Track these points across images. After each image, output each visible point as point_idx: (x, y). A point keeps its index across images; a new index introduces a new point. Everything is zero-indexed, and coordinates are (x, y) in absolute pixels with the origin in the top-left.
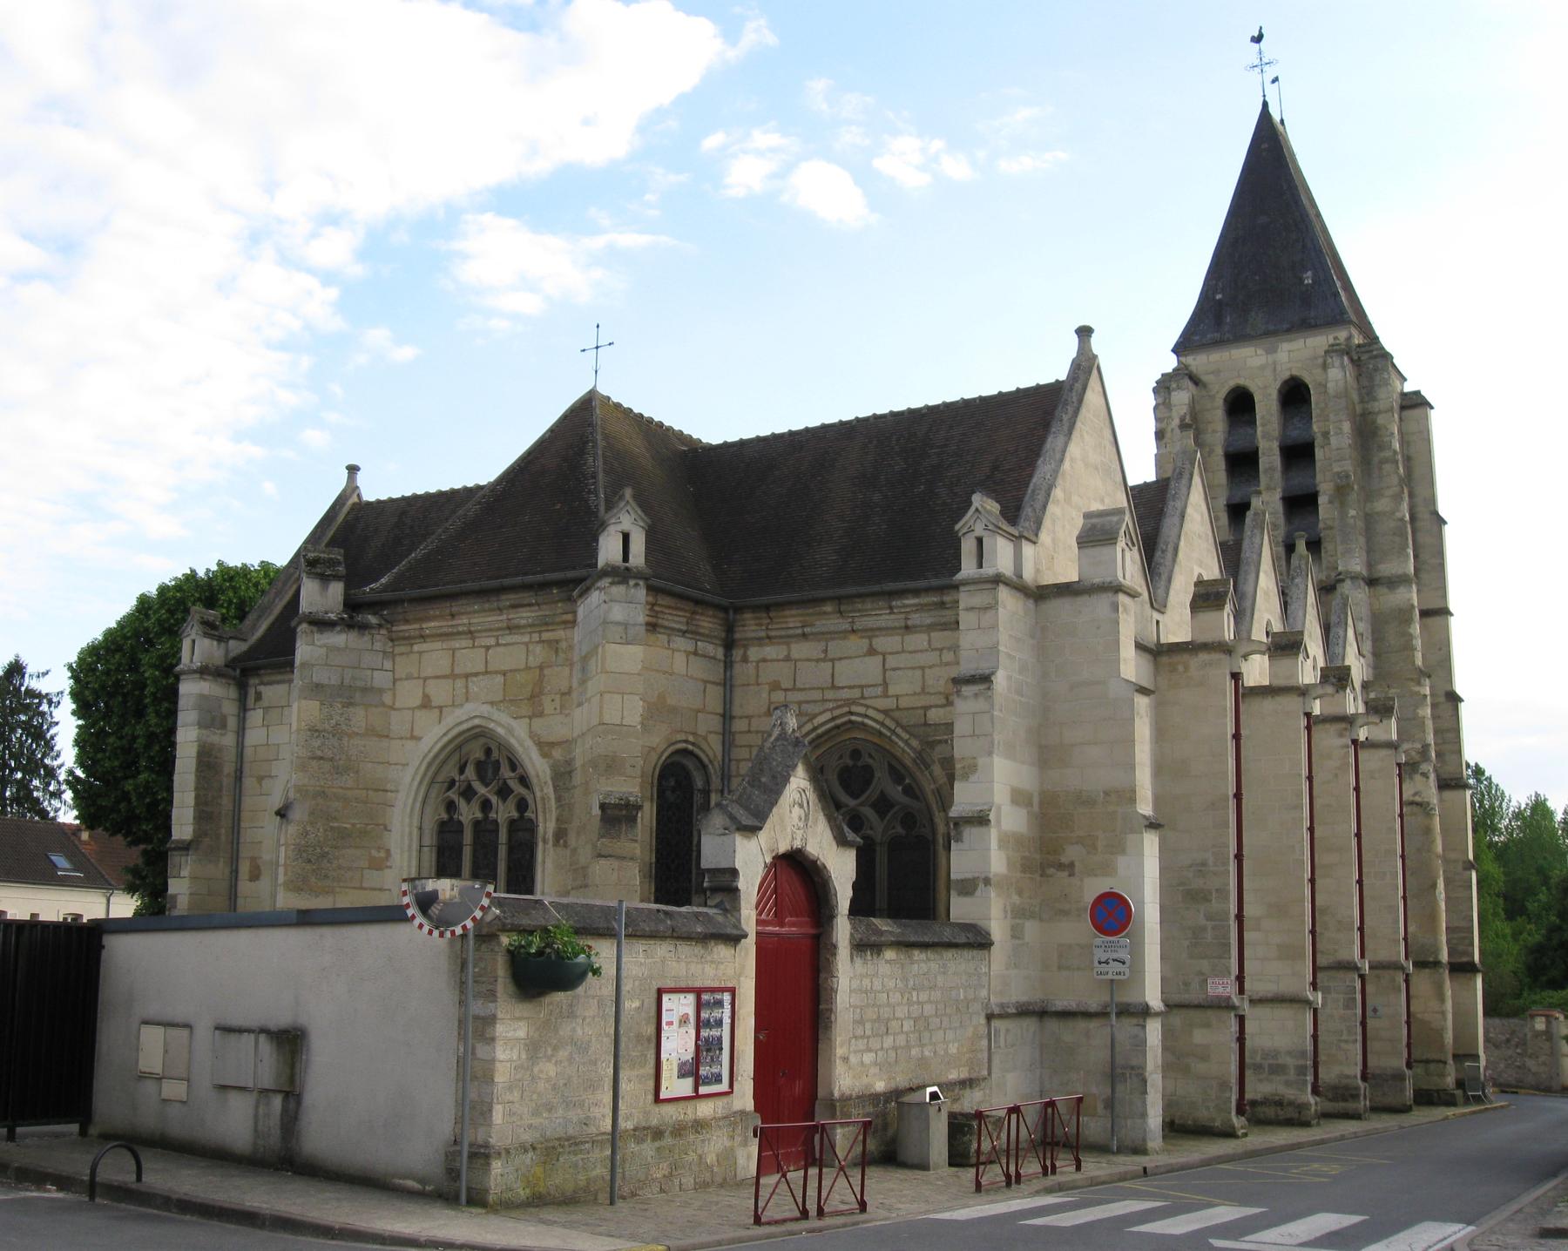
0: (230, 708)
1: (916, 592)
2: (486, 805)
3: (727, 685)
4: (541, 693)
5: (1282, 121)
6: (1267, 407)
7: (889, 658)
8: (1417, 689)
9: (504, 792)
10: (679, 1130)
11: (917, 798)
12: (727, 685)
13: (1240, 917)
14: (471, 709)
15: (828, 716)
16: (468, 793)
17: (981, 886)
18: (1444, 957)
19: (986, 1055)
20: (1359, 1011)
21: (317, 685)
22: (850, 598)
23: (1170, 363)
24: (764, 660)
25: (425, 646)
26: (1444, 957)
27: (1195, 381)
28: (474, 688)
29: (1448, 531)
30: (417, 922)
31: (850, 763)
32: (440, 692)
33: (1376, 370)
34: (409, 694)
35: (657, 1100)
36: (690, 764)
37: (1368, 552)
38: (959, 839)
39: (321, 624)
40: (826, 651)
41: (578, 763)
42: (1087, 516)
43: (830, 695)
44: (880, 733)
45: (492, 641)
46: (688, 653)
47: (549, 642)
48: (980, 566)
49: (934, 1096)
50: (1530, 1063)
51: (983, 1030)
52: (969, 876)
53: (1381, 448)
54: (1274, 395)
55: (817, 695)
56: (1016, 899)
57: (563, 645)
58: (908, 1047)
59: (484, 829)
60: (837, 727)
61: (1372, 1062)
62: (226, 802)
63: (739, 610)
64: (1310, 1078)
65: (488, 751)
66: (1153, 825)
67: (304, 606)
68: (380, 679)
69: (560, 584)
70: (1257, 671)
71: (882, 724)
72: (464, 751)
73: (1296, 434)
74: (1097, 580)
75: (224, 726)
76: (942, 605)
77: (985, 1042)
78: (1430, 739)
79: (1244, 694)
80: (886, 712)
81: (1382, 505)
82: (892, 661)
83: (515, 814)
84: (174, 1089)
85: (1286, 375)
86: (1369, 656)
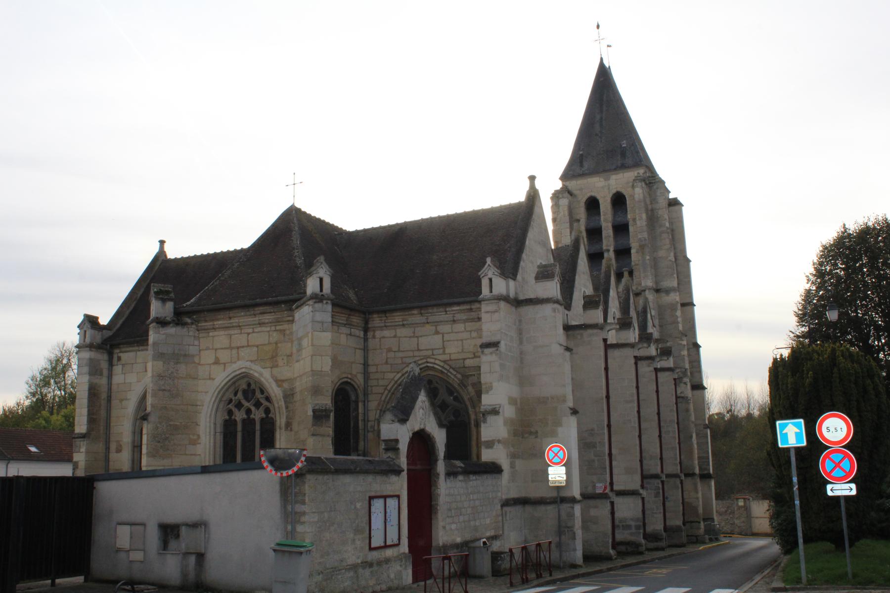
0: (104, 365)
1: (459, 304)
2: (249, 411)
3: (365, 349)
4: (276, 355)
6: (606, 206)
7: (445, 335)
9: (258, 405)
10: (379, 563)
12: (365, 349)
13: (610, 455)
16: (239, 406)
17: (496, 444)
18: (697, 471)
20: (661, 498)
21: (161, 354)
22: (426, 307)
23: (559, 185)
24: (384, 337)
25: (216, 333)
26: (697, 471)
29: (692, 264)
32: (224, 356)
34: (207, 357)
35: (371, 549)
36: (348, 388)
37: (656, 276)
38: (485, 422)
39: (162, 323)
41: (298, 390)
43: (417, 353)
44: (442, 372)
45: (250, 331)
46: (347, 335)
47: (280, 331)
48: (491, 292)
49: (484, 543)
50: (737, 521)
51: (499, 512)
52: (490, 439)
54: (609, 200)
55: (411, 354)
56: (512, 449)
57: (288, 332)
58: (469, 521)
59: (248, 423)
61: (668, 523)
62: (103, 413)
63: (371, 313)
64: (642, 531)
65: (249, 385)
66: (574, 412)
68: (193, 350)
69: (285, 302)
70: (612, 337)
72: (237, 384)
73: (620, 219)
74: (545, 297)
75: (101, 374)
76: (471, 310)
77: (500, 518)
78: (687, 366)
79: (608, 347)
80: (444, 362)
81: (661, 253)
82: (446, 337)
83: (264, 416)
84: (137, 556)
85: (614, 191)
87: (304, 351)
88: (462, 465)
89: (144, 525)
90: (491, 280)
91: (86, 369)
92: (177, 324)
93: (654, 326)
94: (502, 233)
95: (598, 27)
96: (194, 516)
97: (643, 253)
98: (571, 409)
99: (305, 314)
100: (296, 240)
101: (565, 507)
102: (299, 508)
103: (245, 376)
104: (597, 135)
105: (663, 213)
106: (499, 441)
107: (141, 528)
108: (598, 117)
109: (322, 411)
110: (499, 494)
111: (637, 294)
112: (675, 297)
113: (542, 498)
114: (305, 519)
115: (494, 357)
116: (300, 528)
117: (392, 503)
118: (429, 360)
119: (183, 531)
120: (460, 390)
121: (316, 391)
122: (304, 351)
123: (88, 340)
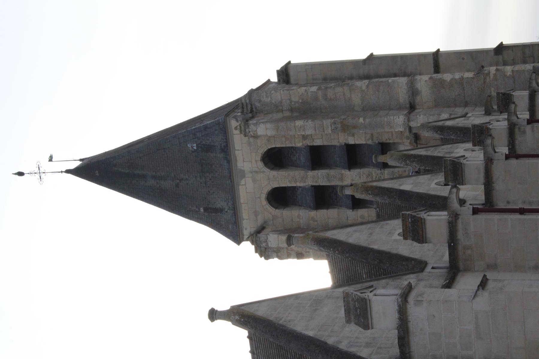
5: (81, 160)
6: (283, 178)
8: (492, 76)
23: (247, 246)
33: (260, 101)
37: (390, 109)
42: (348, 321)
53: (316, 99)
54: (274, 173)
70: (472, 192)
73: (303, 158)
74: (397, 315)
78: (529, 67)
79: (489, 206)
81: (356, 99)
85: (261, 165)
86: (467, 110)
93: (465, 116)
95: (21, 174)
97: (354, 127)
104: (177, 186)
105: (297, 94)
108: (152, 182)
111: (417, 138)
112: (423, 82)
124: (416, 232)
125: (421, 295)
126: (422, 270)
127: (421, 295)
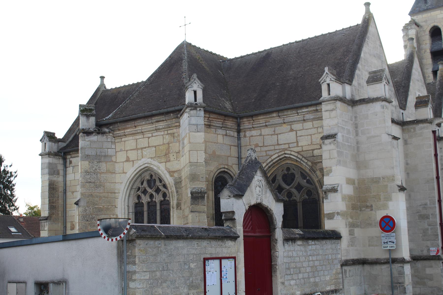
0: (60, 167)
1: (307, 106)
2: (151, 196)
3: (239, 146)
4: (169, 153)
7: (298, 132)
9: (158, 191)
11: (312, 184)
12: (239, 146)
14: (144, 161)
15: (276, 155)
16: (145, 192)
17: (336, 215)
19: (341, 280)
21: (87, 156)
23: (408, 19)
24: (252, 136)
25: (126, 139)
27: (417, 25)
28: (145, 153)
30: (103, 236)
31: (286, 172)
32: (133, 155)
34: (121, 157)
36: (226, 176)
39: (87, 133)
40: (274, 131)
41: (183, 178)
42: (370, 73)
43: (277, 147)
44: (297, 161)
45: (150, 135)
46: (223, 135)
47: (171, 134)
48: (329, 94)
51: (339, 270)
52: (331, 212)
55: (272, 148)
56: (350, 220)
57: (176, 135)
58: (309, 278)
60: (280, 159)
62: (61, 202)
63: (242, 118)
65: (151, 176)
66: (402, 189)
67: (81, 127)
68: (111, 152)
71: (297, 157)
72: (143, 176)
74: (375, 97)
75: (58, 174)
80: (298, 153)
82: (299, 133)
83: (162, 199)
87: (186, 148)
88: (301, 233)
89: (25, 283)
90: (329, 85)
91: (47, 171)
92: (98, 133)
94: (344, 50)
96: (58, 276)
98: (399, 186)
99: (185, 119)
100: (185, 66)
101: (396, 266)
102: (130, 268)
103: (147, 169)
106: (338, 214)
107: (23, 285)
109: (198, 193)
110: (339, 256)
113: (377, 259)
114: (135, 277)
115: (332, 147)
116: (132, 285)
117: (228, 264)
118: (286, 152)
119: (51, 286)
120: (312, 175)
121: (193, 177)
122: (186, 148)
123: (47, 150)
124: (421, 103)
125: (387, 108)
126: (401, 108)
127: (387, 108)
